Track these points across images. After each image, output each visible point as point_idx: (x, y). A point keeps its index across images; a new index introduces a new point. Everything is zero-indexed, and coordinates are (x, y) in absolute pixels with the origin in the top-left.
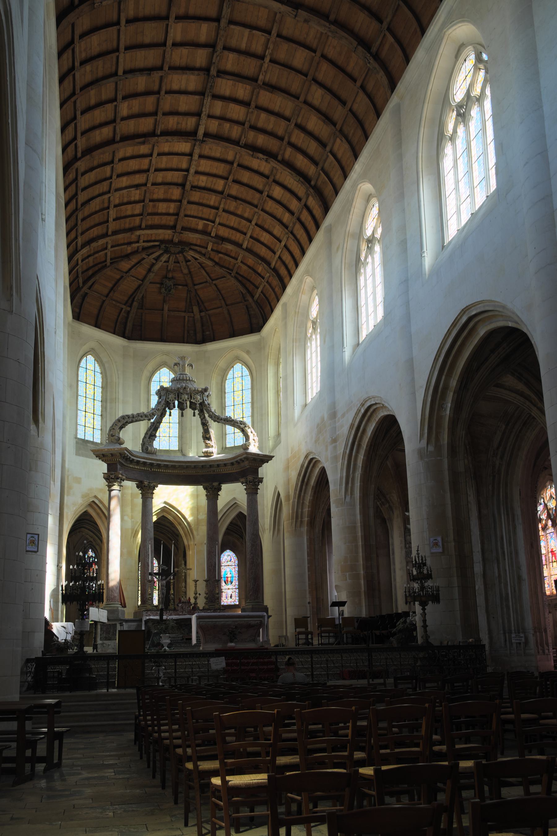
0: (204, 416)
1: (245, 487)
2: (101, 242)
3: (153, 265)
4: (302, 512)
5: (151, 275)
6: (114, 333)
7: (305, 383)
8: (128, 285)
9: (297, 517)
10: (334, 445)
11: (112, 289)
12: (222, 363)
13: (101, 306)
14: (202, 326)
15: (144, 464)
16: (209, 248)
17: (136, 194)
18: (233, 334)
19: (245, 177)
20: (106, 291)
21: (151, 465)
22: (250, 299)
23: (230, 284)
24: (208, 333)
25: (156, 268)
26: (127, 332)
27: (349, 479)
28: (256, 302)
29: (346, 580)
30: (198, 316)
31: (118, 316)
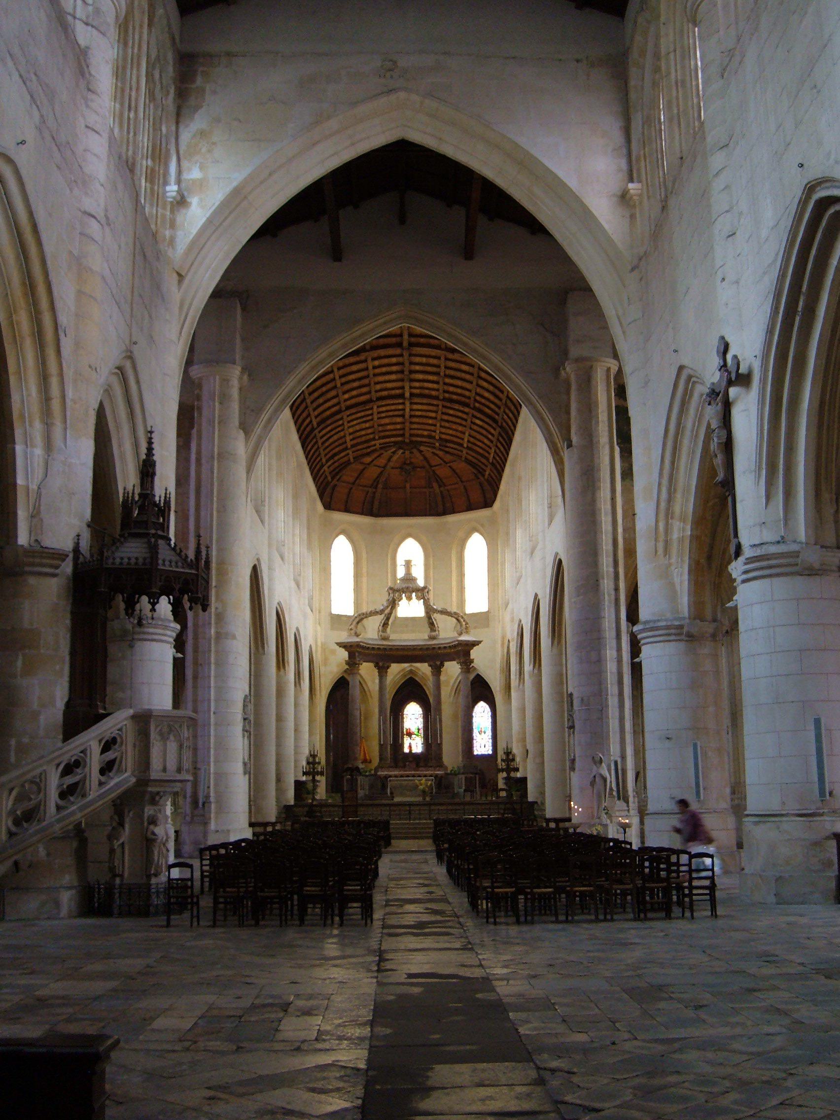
2: (342, 454)
3: (391, 457)
5: (391, 464)
6: (362, 513)
8: (372, 472)
11: (357, 478)
12: (461, 534)
13: (349, 493)
14: (443, 497)
15: (379, 649)
16: (437, 444)
17: (367, 425)
18: (470, 508)
19: (451, 412)
20: (352, 480)
21: (385, 649)
22: (482, 478)
23: (460, 466)
25: (395, 458)
28: (487, 480)
30: (437, 490)
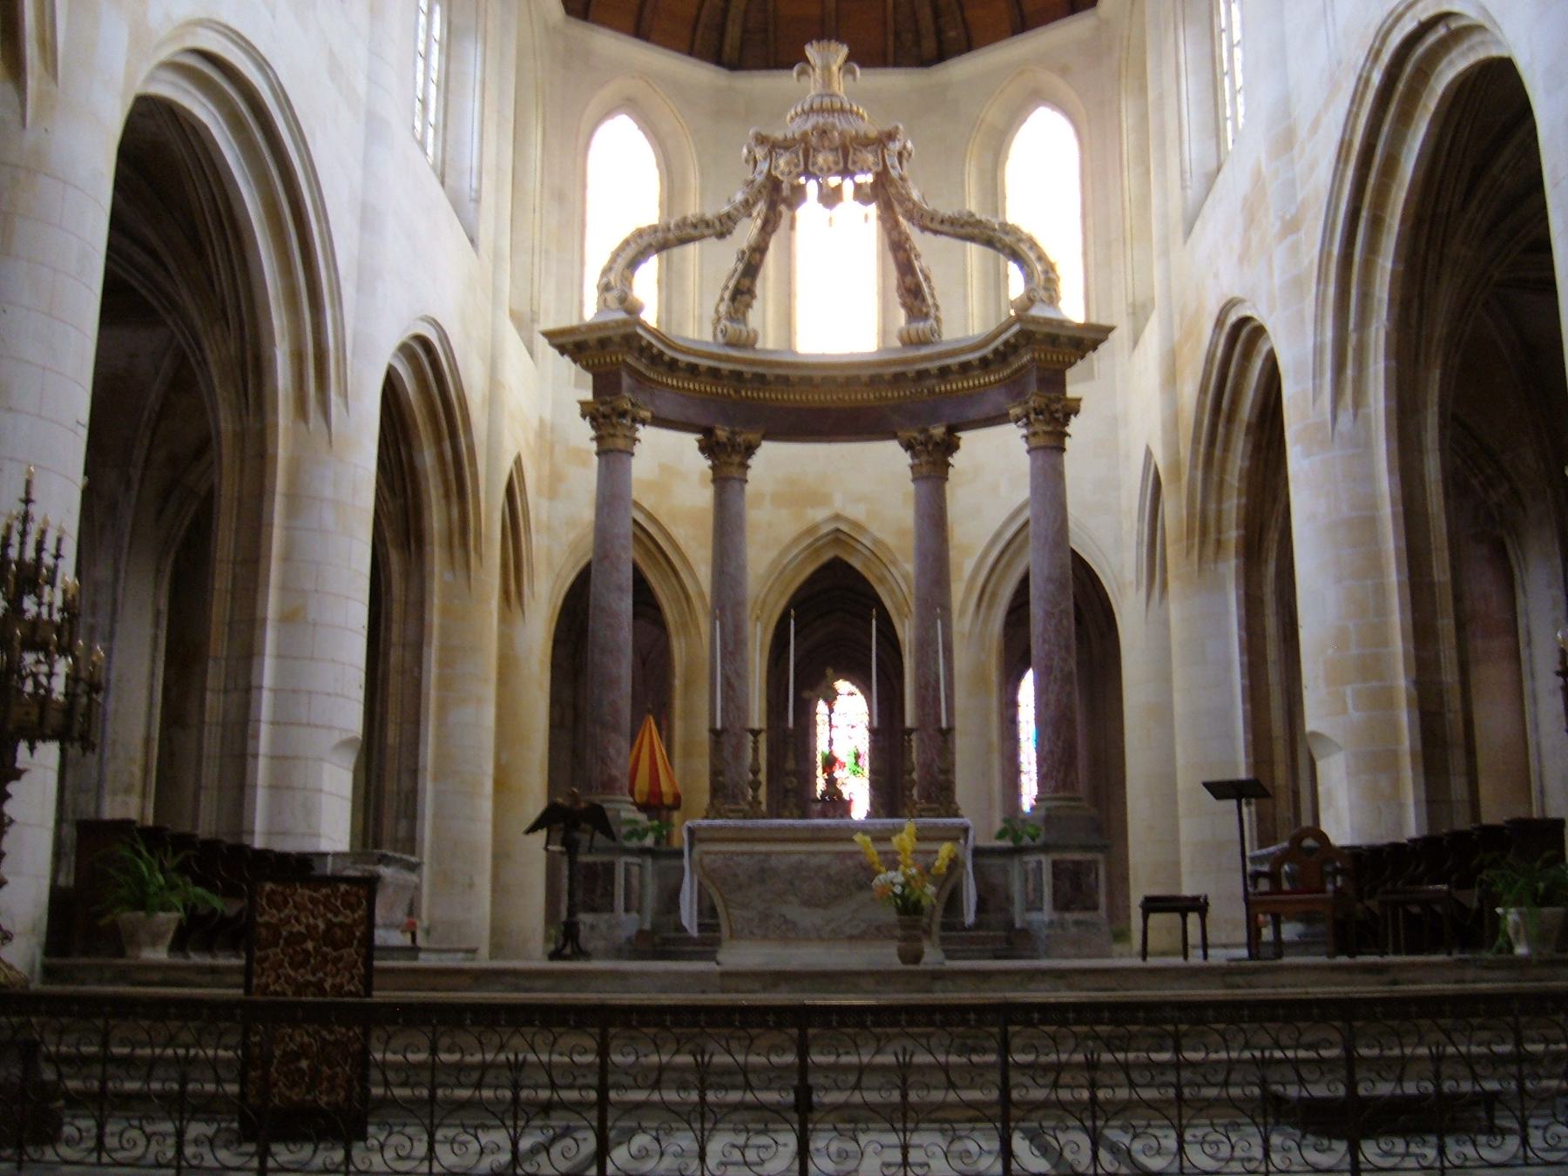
0: (897, 224)
1: (1024, 431)
4: (1219, 513)
7: (1216, 105)
9: (1203, 530)
10: (1291, 239)
12: (993, 114)
15: (715, 373)
21: (738, 375)
24: (952, 34)
26: (727, 48)
27: (1343, 357)
29: (1345, 711)
31: (700, 9)
